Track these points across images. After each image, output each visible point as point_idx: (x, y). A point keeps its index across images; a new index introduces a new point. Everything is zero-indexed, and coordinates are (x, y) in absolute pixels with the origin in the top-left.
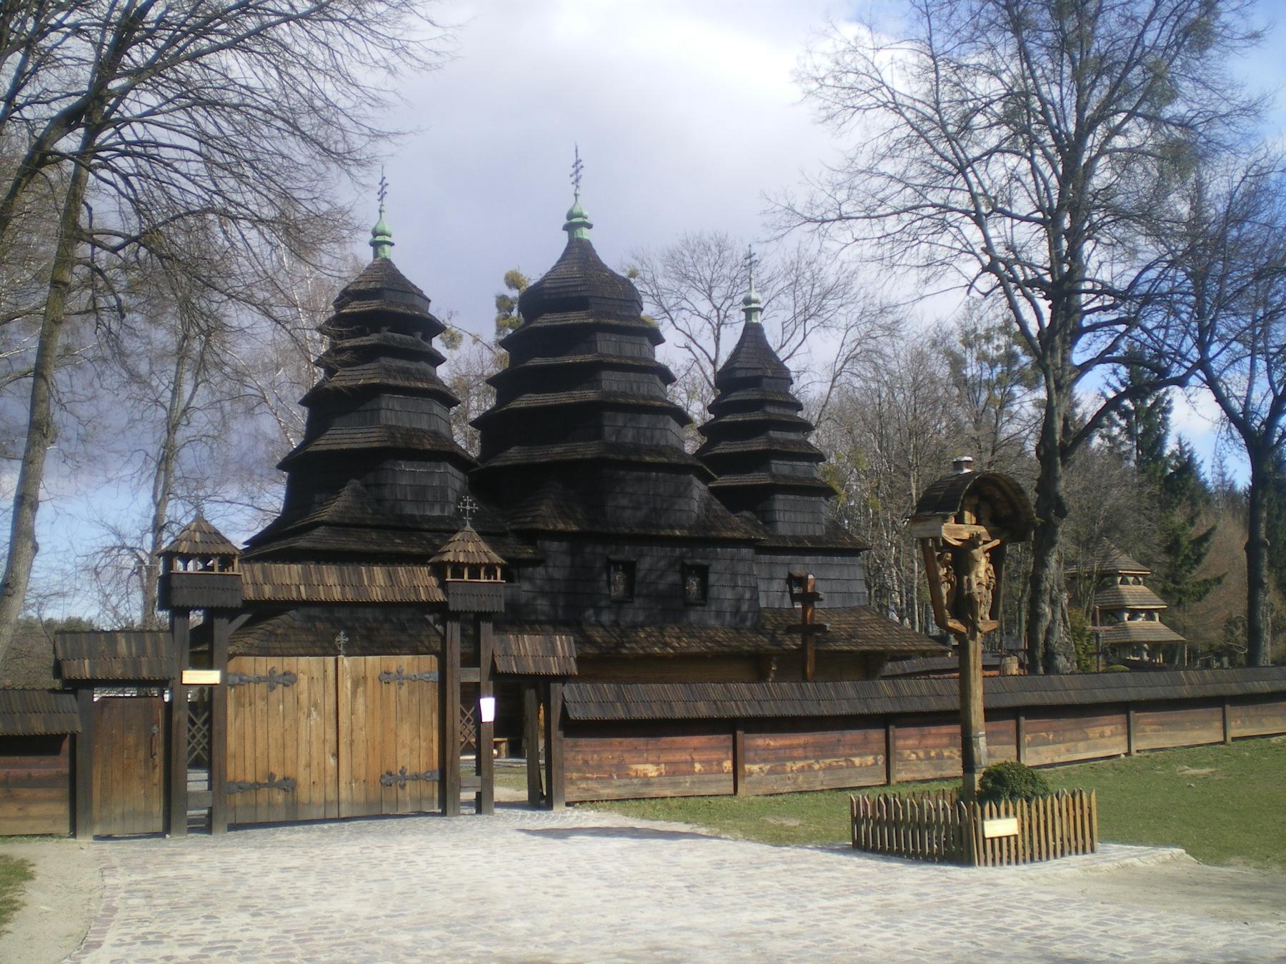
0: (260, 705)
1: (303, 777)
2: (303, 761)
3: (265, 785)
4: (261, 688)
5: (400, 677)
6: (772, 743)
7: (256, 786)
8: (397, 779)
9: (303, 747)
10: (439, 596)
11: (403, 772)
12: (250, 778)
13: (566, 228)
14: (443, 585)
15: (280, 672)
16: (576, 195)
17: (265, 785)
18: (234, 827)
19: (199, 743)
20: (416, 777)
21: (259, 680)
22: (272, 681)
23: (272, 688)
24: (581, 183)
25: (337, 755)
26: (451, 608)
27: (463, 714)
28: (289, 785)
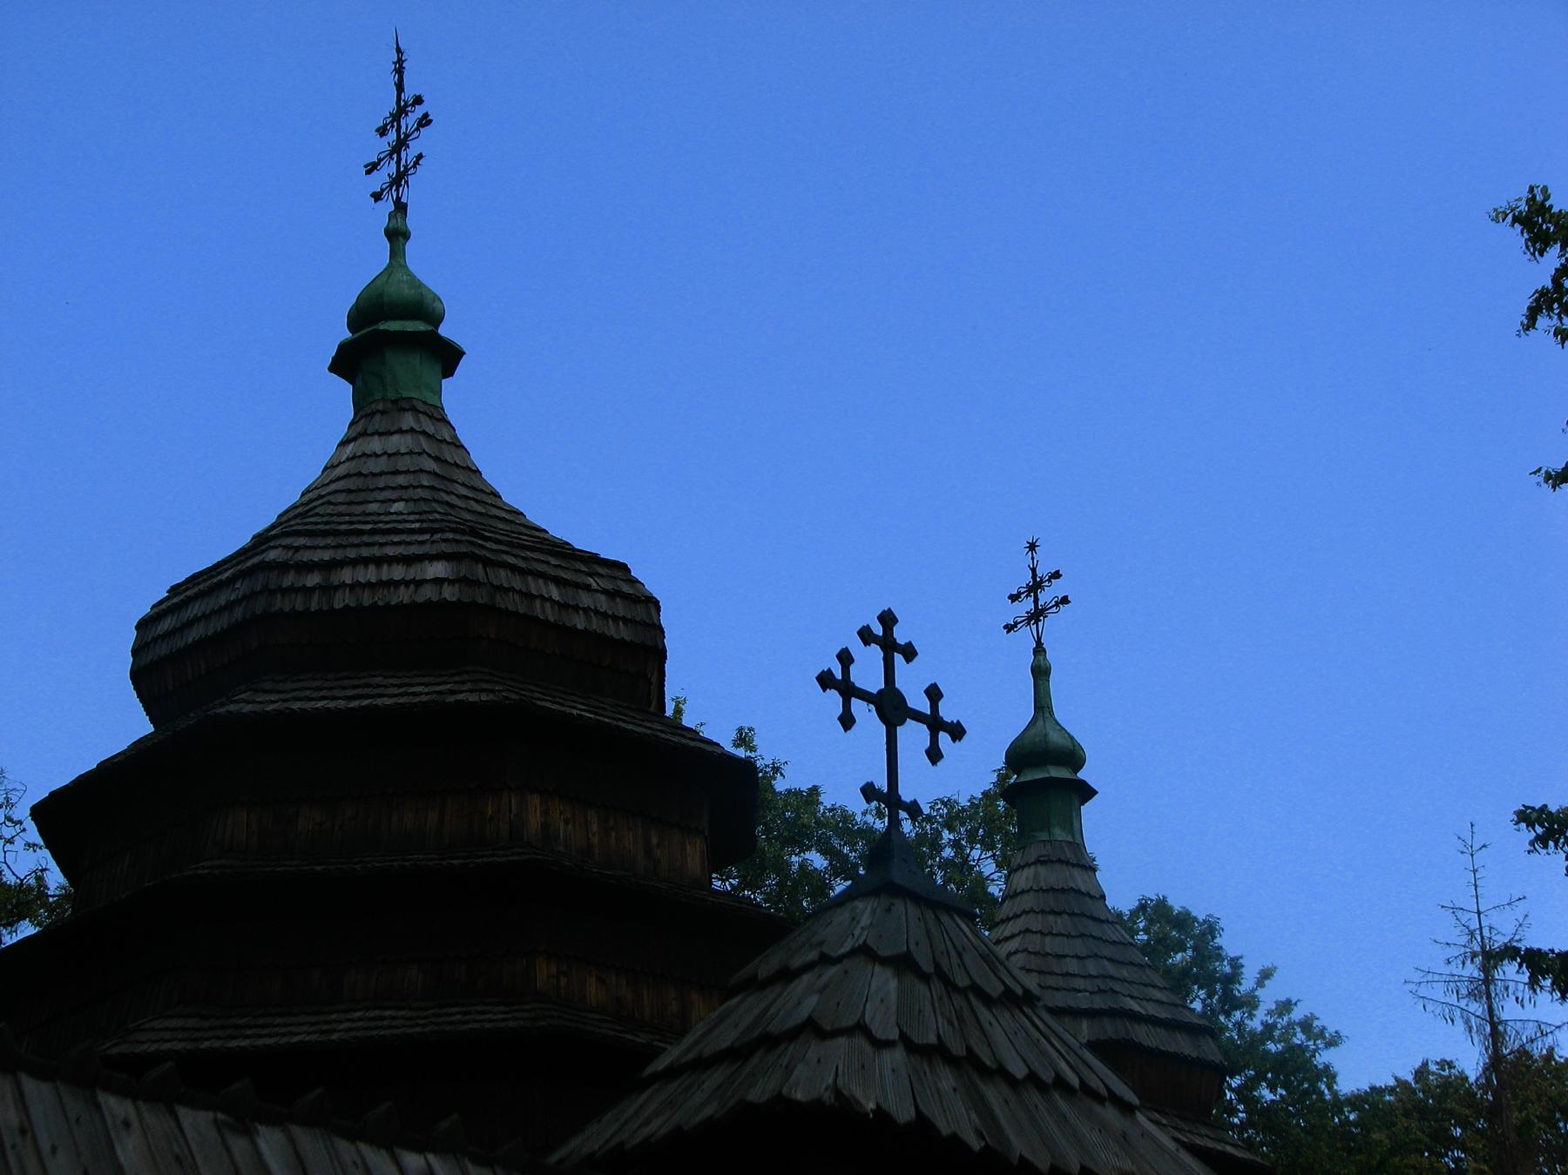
13: (345, 363)
16: (397, 235)
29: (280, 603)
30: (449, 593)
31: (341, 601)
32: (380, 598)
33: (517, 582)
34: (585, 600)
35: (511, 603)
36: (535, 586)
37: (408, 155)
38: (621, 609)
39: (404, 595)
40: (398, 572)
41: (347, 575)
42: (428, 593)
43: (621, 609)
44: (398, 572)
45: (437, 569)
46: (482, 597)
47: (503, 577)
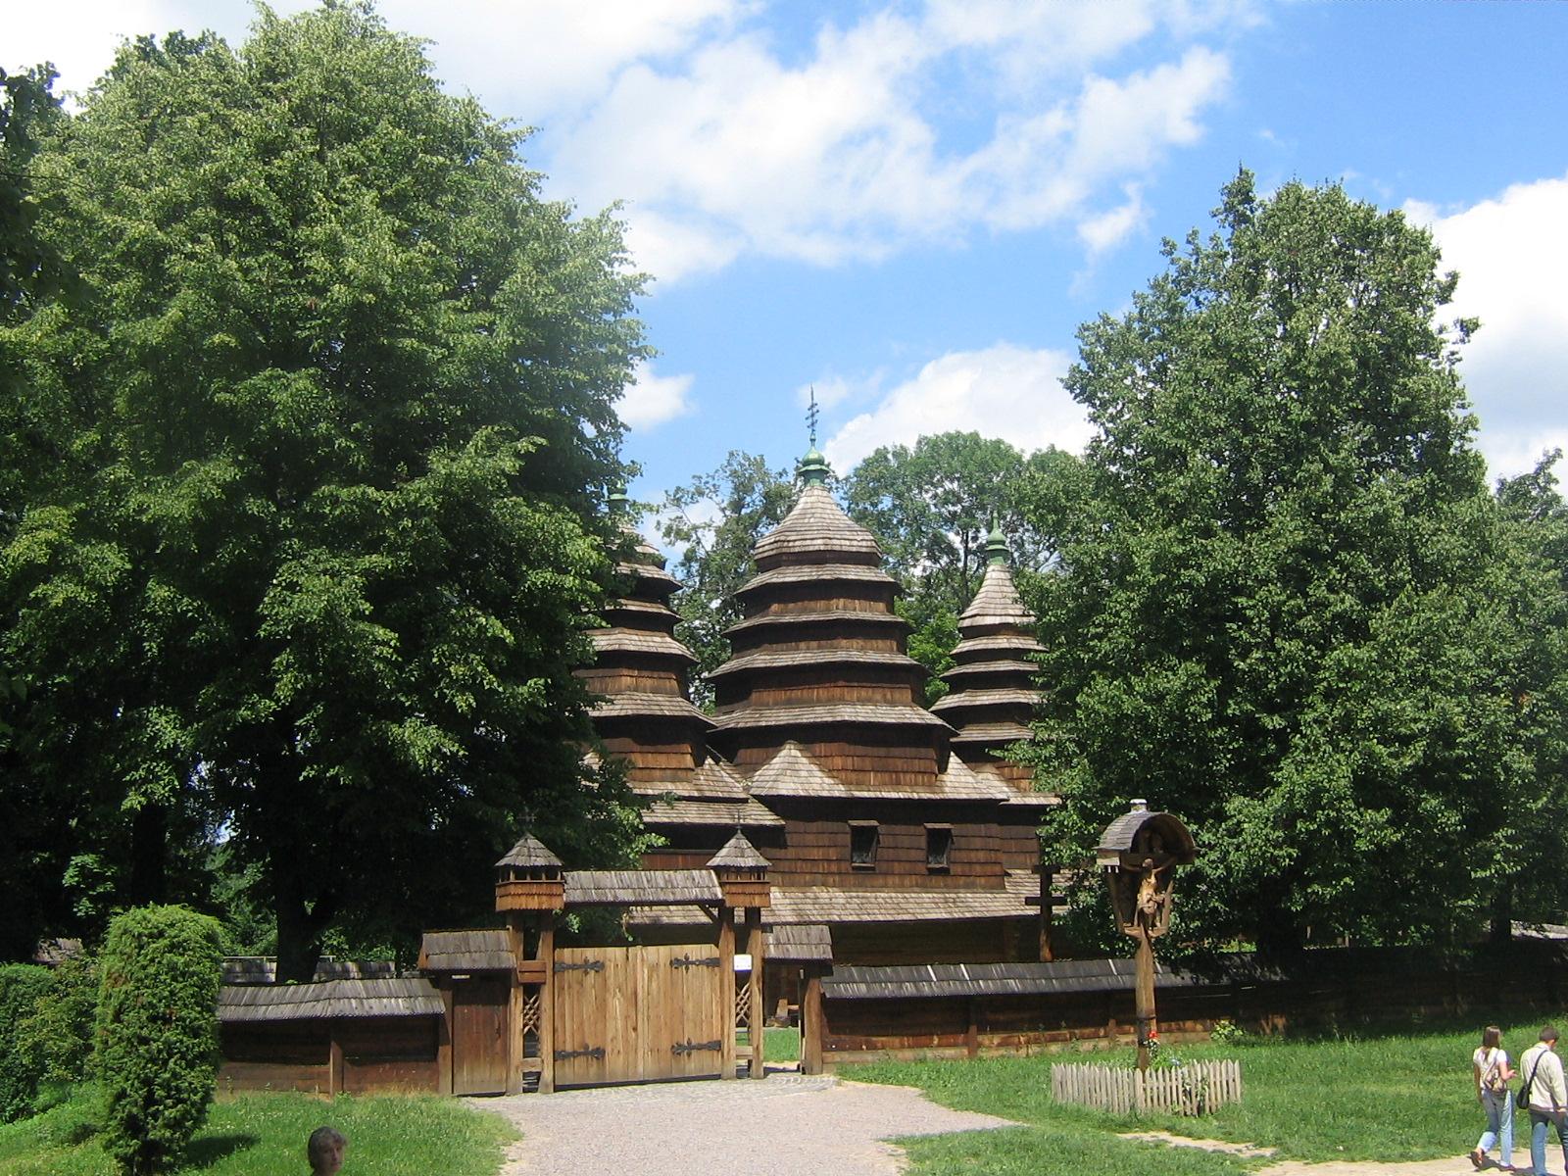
0: (576, 987)
1: (608, 1050)
2: (610, 1036)
3: (579, 1054)
4: (578, 973)
5: (687, 962)
6: (1002, 1018)
7: (575, 1054)
8: (685, 1048)
9: (610, 1025)
10: (720, 896)
11: (689, 1043)
12: (569, 1048)
14: (722, 885)
15: (592, 960)
16: (813, 440)
17: (579, 1054)
18: (557, 1089)
19: (530, 1019)
20: (700, 1047)
21: (574, 967)
22: (586, 967)
23: (586, 973)
24: (817, 427)
25: (635, 1029)
26: (728, 904)
27: (737, 994)
28: (599, 1054)
29: (784, 550)
30: (822, 548)
31: (797, 550)
32: (807, 549)
33: (838, 542)
34: (855, 543)
35: (837, 548)
36: (843, 542)
37: (815, 418)
38: (864, 543)
39: (811, 548)
40: (808, 542)
41: (797, 543)
42: (816, 548)
43: (864, 543)
44: (808, 542)
45: (819, 542)
46: (829, 548)
47: (835, 542)
